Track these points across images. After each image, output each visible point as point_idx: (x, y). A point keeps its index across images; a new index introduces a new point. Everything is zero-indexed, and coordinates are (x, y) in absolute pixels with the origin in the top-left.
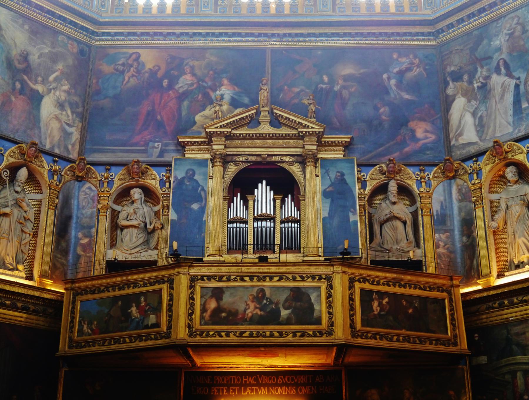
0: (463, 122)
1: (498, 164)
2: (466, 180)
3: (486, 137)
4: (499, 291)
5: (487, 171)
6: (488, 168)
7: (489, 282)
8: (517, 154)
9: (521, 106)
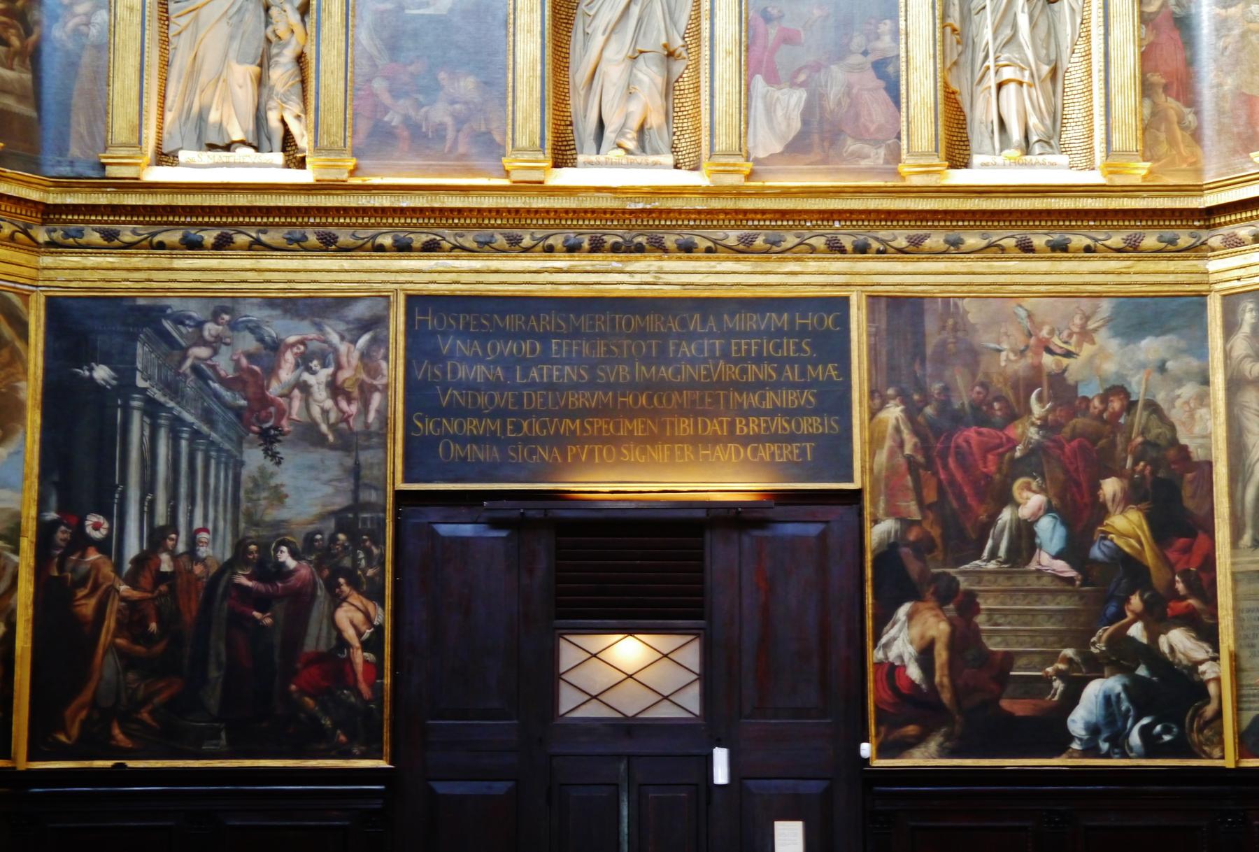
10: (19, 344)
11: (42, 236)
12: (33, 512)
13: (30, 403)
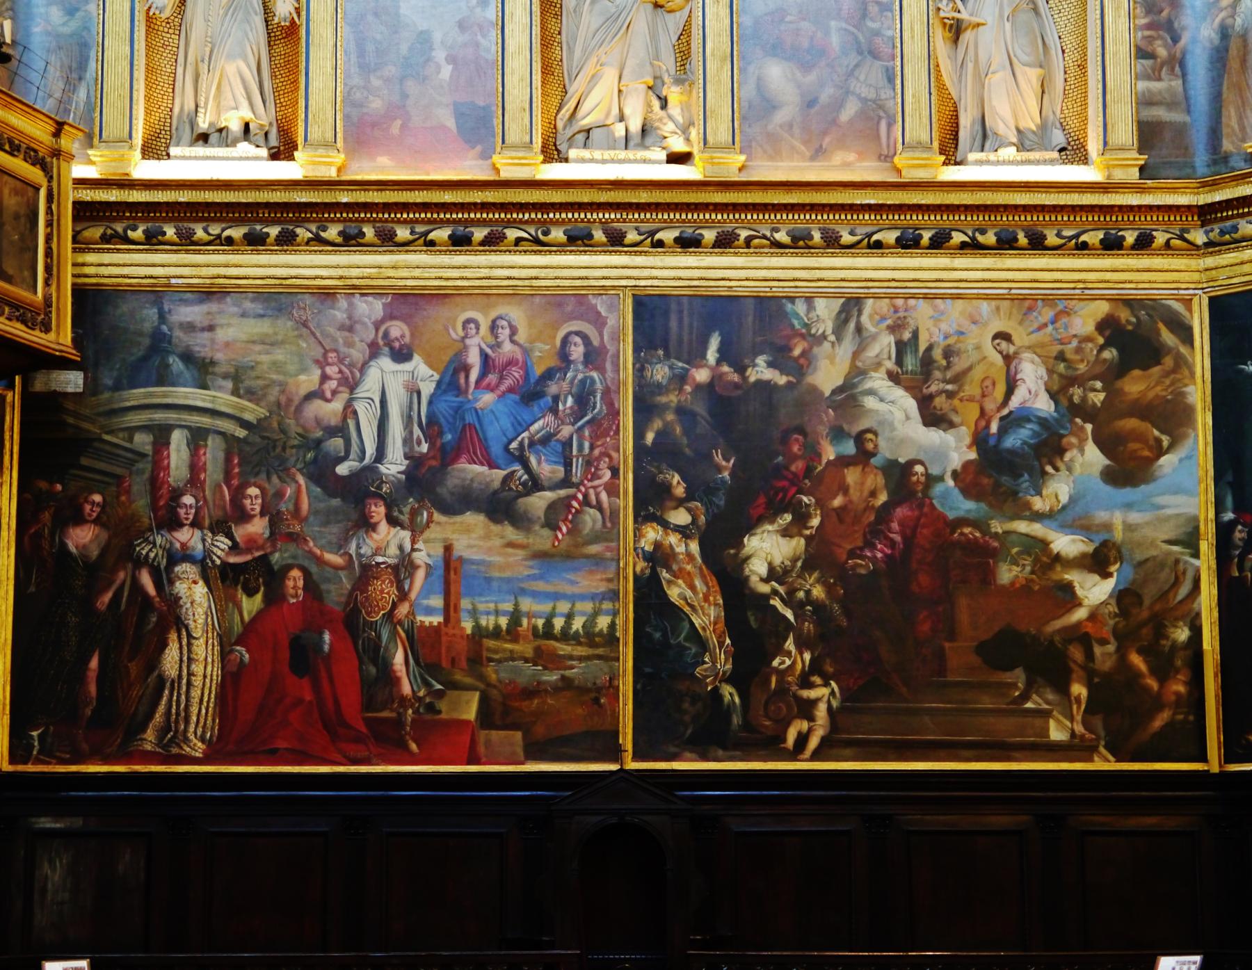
7: (121, 159)
10: (1183, 350)
11: (1199, 237)
12: (1212, 514)
13: (1199, 407)
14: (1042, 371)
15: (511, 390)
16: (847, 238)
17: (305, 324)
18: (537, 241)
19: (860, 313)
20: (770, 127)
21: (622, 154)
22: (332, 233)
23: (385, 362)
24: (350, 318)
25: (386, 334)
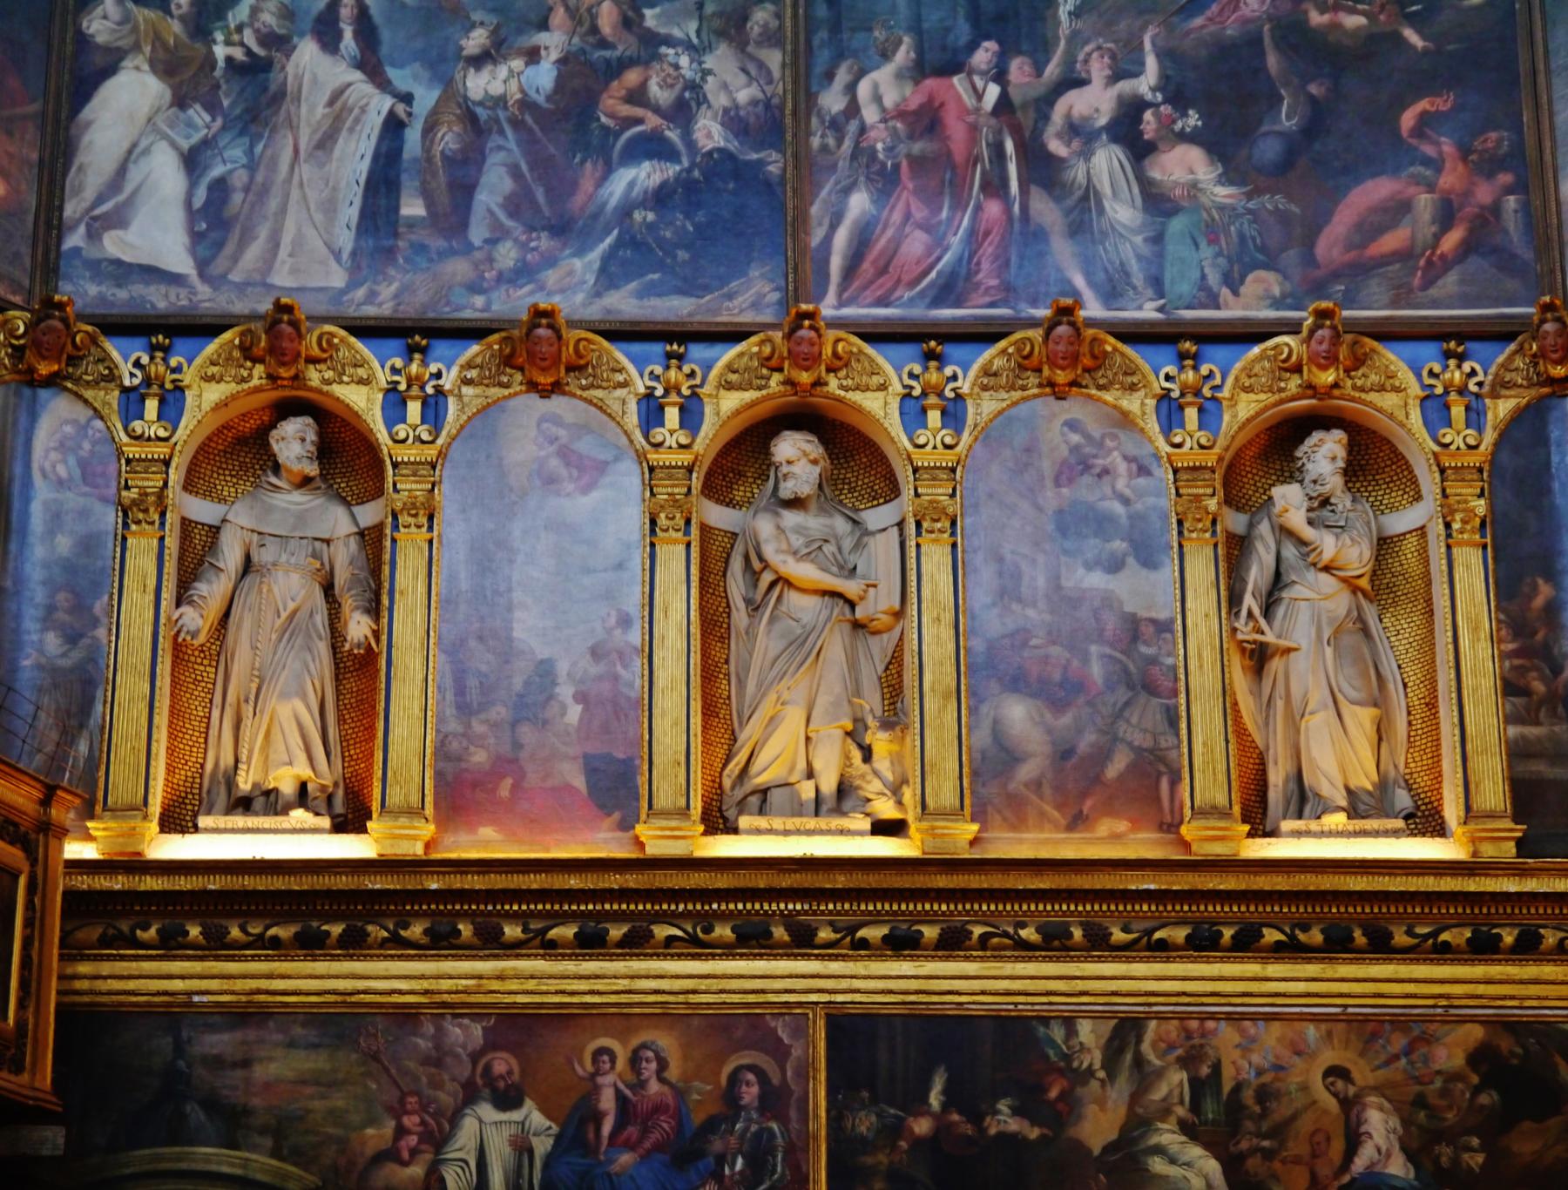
0: (134, 176)
1: (257, 390)
2: (105, 412)
3: (229, 270)
4: (184, 883)
5: (206, 406)
6: (214, 393)
7: (132, 833)
8: (345, 379)
9: (397, 209)
14: (1394, 1122)
15: (658, 1147)
16: (1118, 936)
17: (375, 1057)
18: (694, 941)
19: (1139, 1040)
20: (1012, 786)
21: (812, 823)
22: (416, 931)
23: (487, 1111)
24: (437, 1047)
25: (488, 1069)
